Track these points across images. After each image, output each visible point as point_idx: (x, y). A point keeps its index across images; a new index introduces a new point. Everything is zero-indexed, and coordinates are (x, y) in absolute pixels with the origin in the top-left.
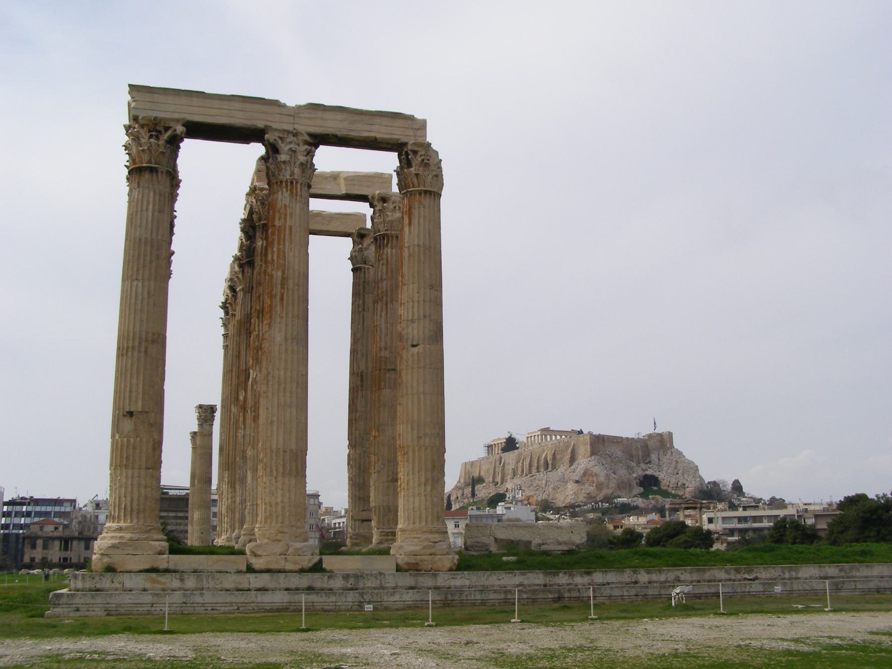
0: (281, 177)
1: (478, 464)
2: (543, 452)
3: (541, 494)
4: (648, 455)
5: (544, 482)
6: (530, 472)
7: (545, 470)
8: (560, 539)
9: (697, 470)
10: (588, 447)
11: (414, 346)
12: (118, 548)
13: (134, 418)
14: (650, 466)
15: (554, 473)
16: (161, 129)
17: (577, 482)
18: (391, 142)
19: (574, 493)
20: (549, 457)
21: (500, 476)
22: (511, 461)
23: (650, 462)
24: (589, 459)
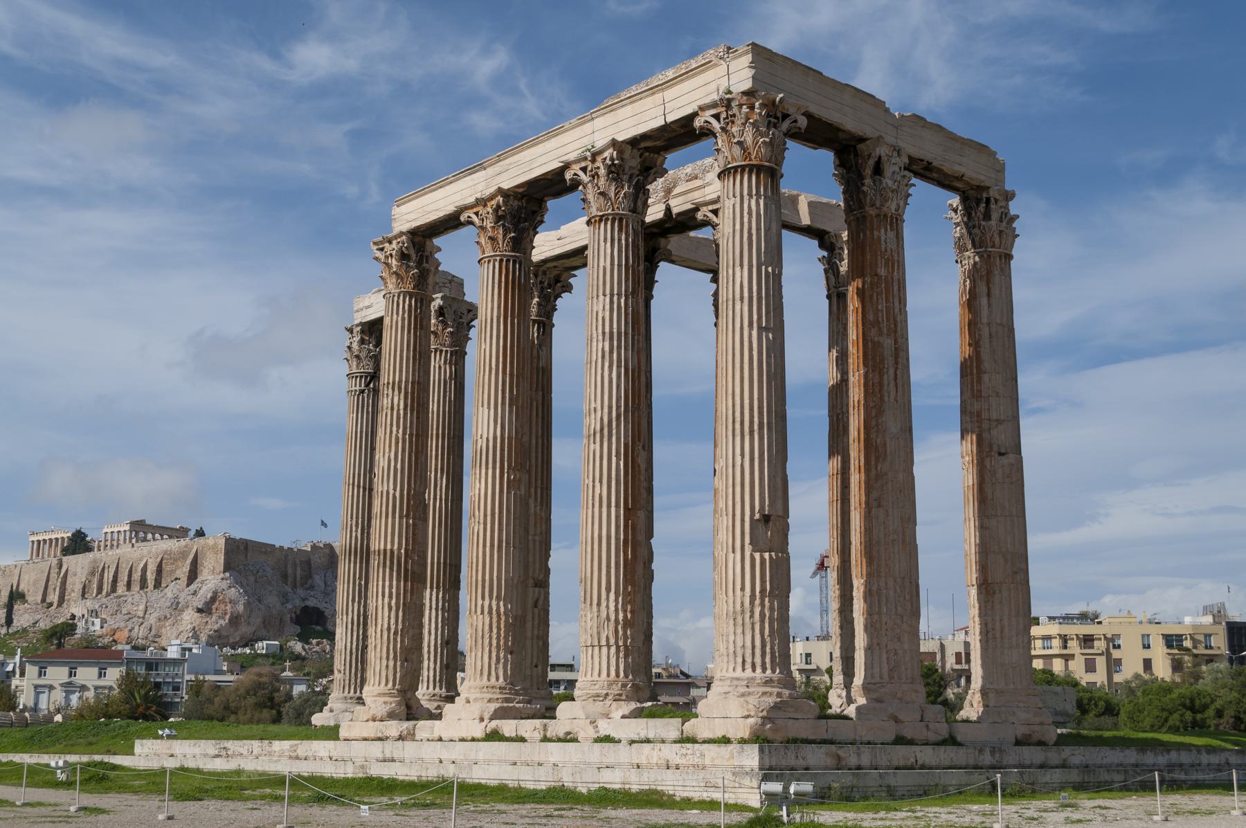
0: (885, 209)
1: (17, 571)
2: (141, 560)
3: (137, 628)
4: (309, 576)
5: (142, 607)
6: (114, 588)
7: (141, 589)
8: (1058, 709)
11: (1000, 454)
12: (780, 708)
13: (771, 523)
14: (312, 593)
16: (779, 115)
17: (199, 611)
18: (974, 183)
19: (194, 628)
20: (152, 568)
22: (79, 570)
23: (312, 587)
24: (222, 575)
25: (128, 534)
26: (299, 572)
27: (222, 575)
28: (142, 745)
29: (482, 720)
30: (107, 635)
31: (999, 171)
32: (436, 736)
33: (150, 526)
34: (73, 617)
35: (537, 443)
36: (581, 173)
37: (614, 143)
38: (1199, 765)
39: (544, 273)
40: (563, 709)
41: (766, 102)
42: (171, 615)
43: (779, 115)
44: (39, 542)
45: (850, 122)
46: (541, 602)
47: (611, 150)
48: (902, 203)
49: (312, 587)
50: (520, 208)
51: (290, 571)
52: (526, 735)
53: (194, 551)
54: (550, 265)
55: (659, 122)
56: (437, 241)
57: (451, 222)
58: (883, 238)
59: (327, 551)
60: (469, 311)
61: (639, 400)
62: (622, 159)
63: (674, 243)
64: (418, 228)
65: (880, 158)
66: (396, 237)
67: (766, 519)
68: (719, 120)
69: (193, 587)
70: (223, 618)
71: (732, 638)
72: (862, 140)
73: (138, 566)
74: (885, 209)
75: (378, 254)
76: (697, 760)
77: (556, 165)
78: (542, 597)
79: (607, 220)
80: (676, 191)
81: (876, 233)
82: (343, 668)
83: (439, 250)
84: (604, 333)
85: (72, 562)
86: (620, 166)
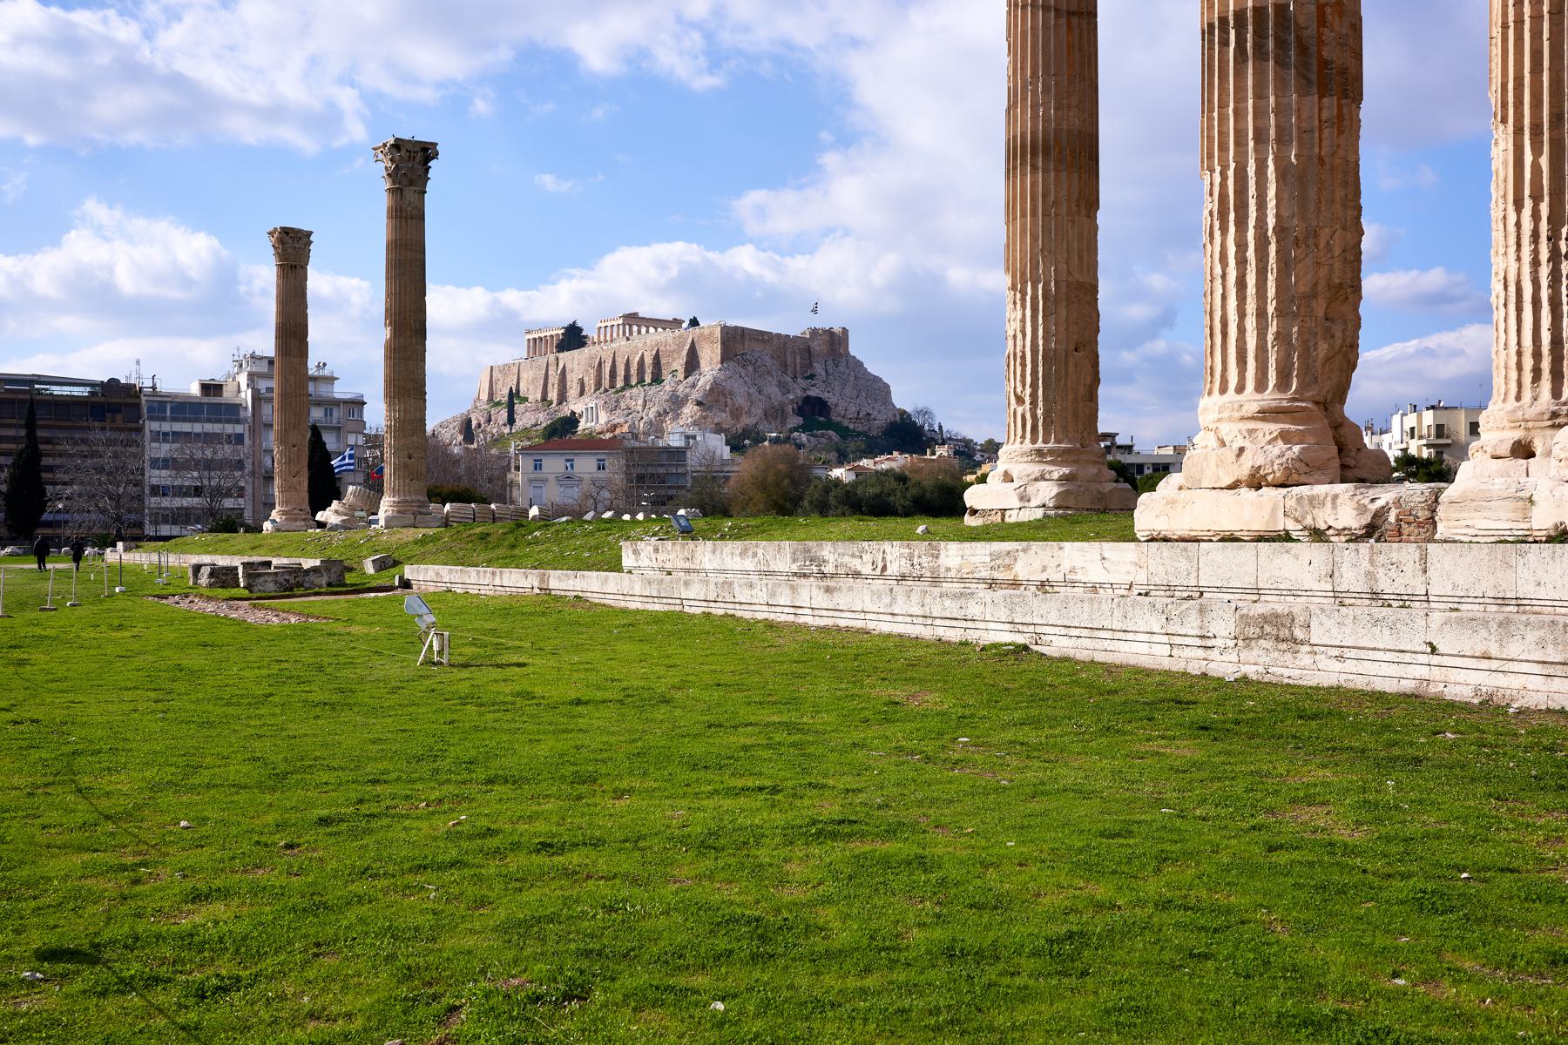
5: (640, 402)
9: (889, 392)
15: (654, 389)
20: (648, 361)
21: (556, 391)
23: (812, 377)
25: (621, 327)
26: (798, 360)
27: (719, 366)
28: (636, 552)
30: (608, 431)
33: (643, 318)
34: (573, 413)
44: (535, 340)
51: (789, 359)
53: (690, 340)
59: (826, 337)
69: (690, 379)
70: (725, 412)
73: (634, 357)
82: (1028, 390)
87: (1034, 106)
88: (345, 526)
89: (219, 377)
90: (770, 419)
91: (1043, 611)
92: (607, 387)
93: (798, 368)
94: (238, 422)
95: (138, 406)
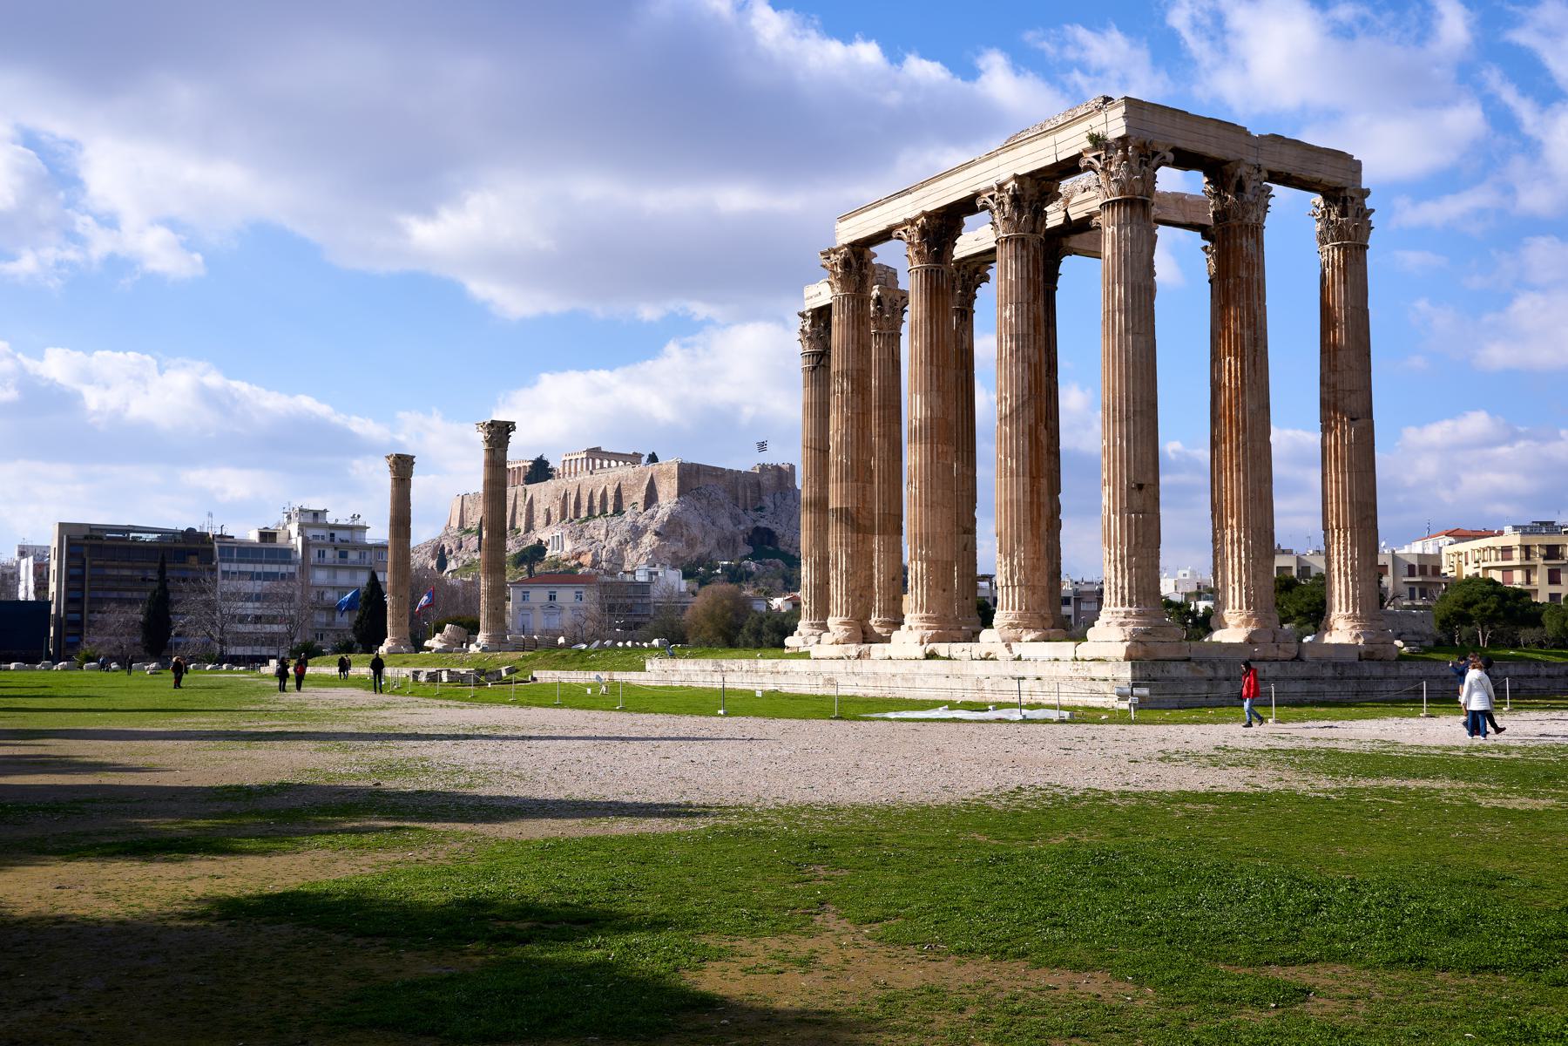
5: (603, 531)
6: (577, 516)
10: (675, 483)
13: (1144, 491)
15: (616, 520)
16: (1150, 154)
20: (611, 493)
21: (524, 520)
23: (761, 509)
26: (748, 494)
29: (922, 643)
31: (1355, 172)
32: (887, 656)
34: (540, 541)
35: (962, 414)
36: (989, 200)
37: (1016, 177)
38: (1538, 676)
39: (965, 267)
40: (985, 634)
41: (1137, 144)
42: (632, 539)
43: (1150, 154)
45: (1213, 151)
46: (969, 546)
47: (1013, 182)
48: (1261, 214)
49: (761, 509)
50: (941, 226)
51: (740, 493)
52: (954, 655)
54: (971, 260)
55: (1052, 161)
56: (873, 249)
57: (885, 236)
58: (1244, 245)
59: (775, 473)
60: (903, 298)
61: (1041, 388)
62: (1023, 189)
63: (1075, 241)
64: (857, 241)
65: (1241, 177)
66: (840, 249)
67: (1140, 487)
68: (1099, 161)
69: (650, 511)
71: (1113, 580)
72: (1226, 162)
74: (1246, 220)
75: (826, 262)
76: (1085, 674)
77: (968, 193)
78: (970, 543)
79: (1011, 240)
80: (1073, 201)
81: (1238, 241)
83: (875, 255)
84: (1011, 335)
85: (533, 489)
86: (1022, 195)
87: (811, 487)
88: (444, 651)
89: (272, 527)
90: (723, 548)
91: (781, 679)
92: (572, 517)
93: (749, 499)
94: (290, 563)
95: (212, 550)
